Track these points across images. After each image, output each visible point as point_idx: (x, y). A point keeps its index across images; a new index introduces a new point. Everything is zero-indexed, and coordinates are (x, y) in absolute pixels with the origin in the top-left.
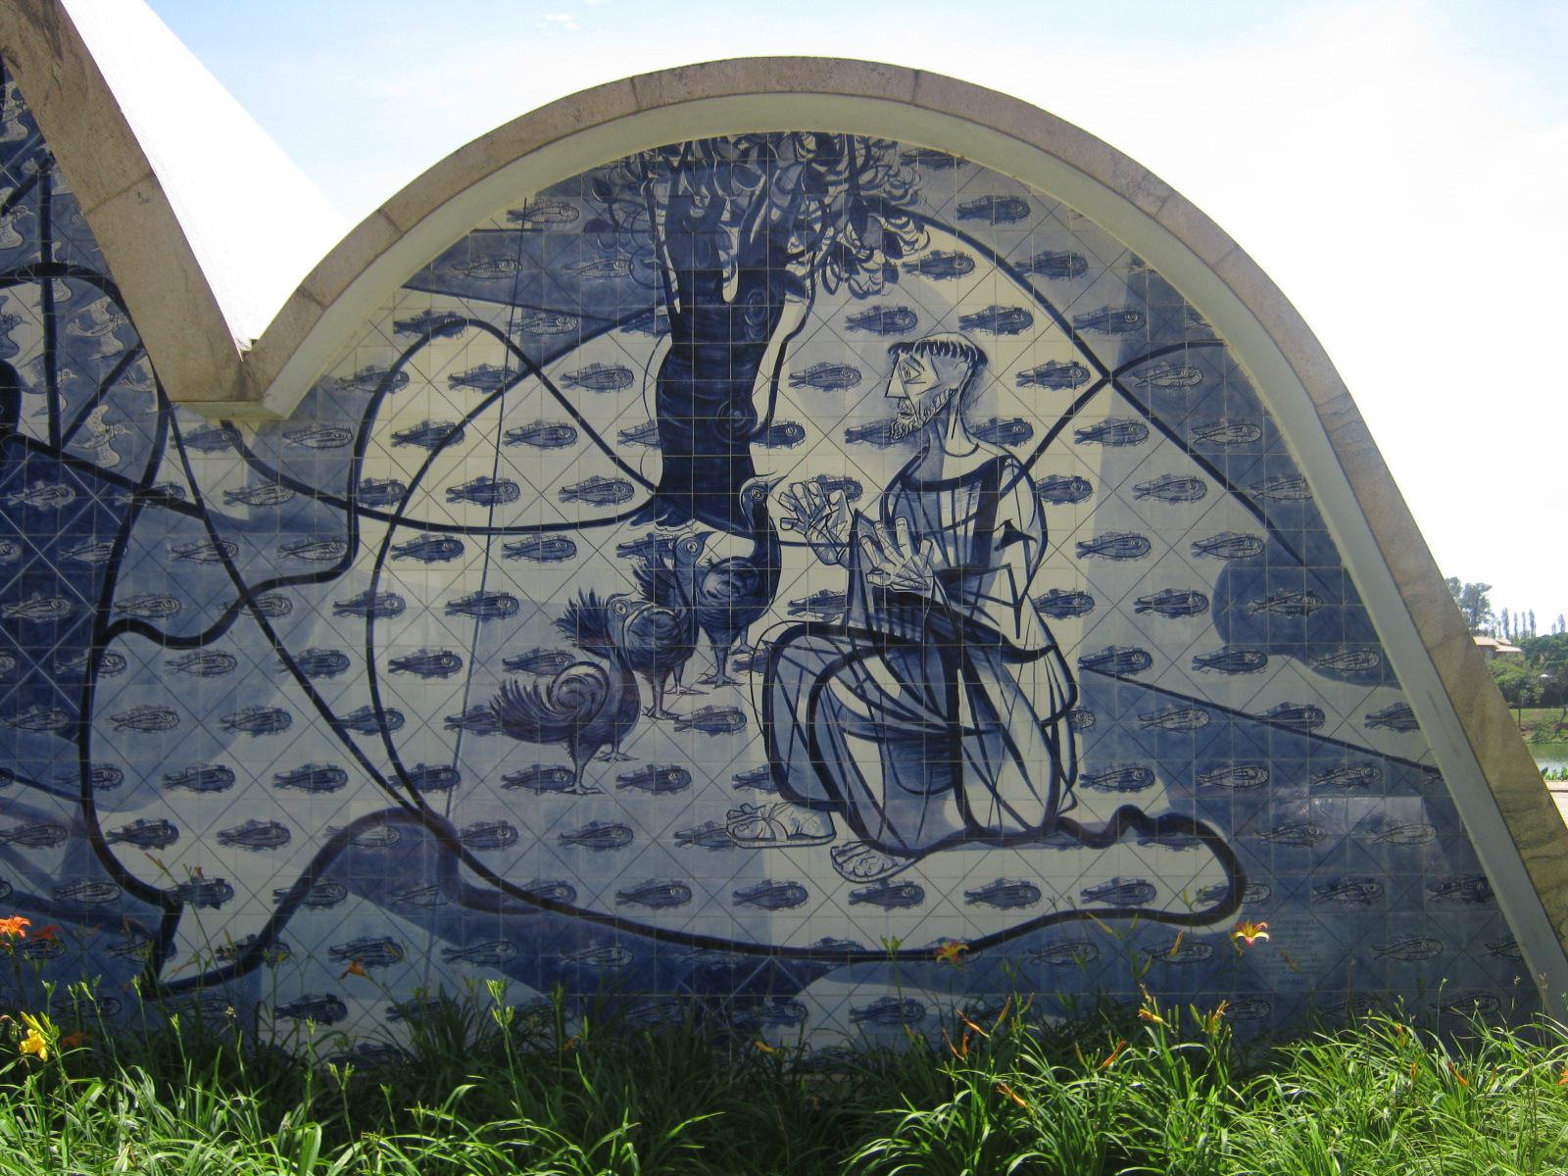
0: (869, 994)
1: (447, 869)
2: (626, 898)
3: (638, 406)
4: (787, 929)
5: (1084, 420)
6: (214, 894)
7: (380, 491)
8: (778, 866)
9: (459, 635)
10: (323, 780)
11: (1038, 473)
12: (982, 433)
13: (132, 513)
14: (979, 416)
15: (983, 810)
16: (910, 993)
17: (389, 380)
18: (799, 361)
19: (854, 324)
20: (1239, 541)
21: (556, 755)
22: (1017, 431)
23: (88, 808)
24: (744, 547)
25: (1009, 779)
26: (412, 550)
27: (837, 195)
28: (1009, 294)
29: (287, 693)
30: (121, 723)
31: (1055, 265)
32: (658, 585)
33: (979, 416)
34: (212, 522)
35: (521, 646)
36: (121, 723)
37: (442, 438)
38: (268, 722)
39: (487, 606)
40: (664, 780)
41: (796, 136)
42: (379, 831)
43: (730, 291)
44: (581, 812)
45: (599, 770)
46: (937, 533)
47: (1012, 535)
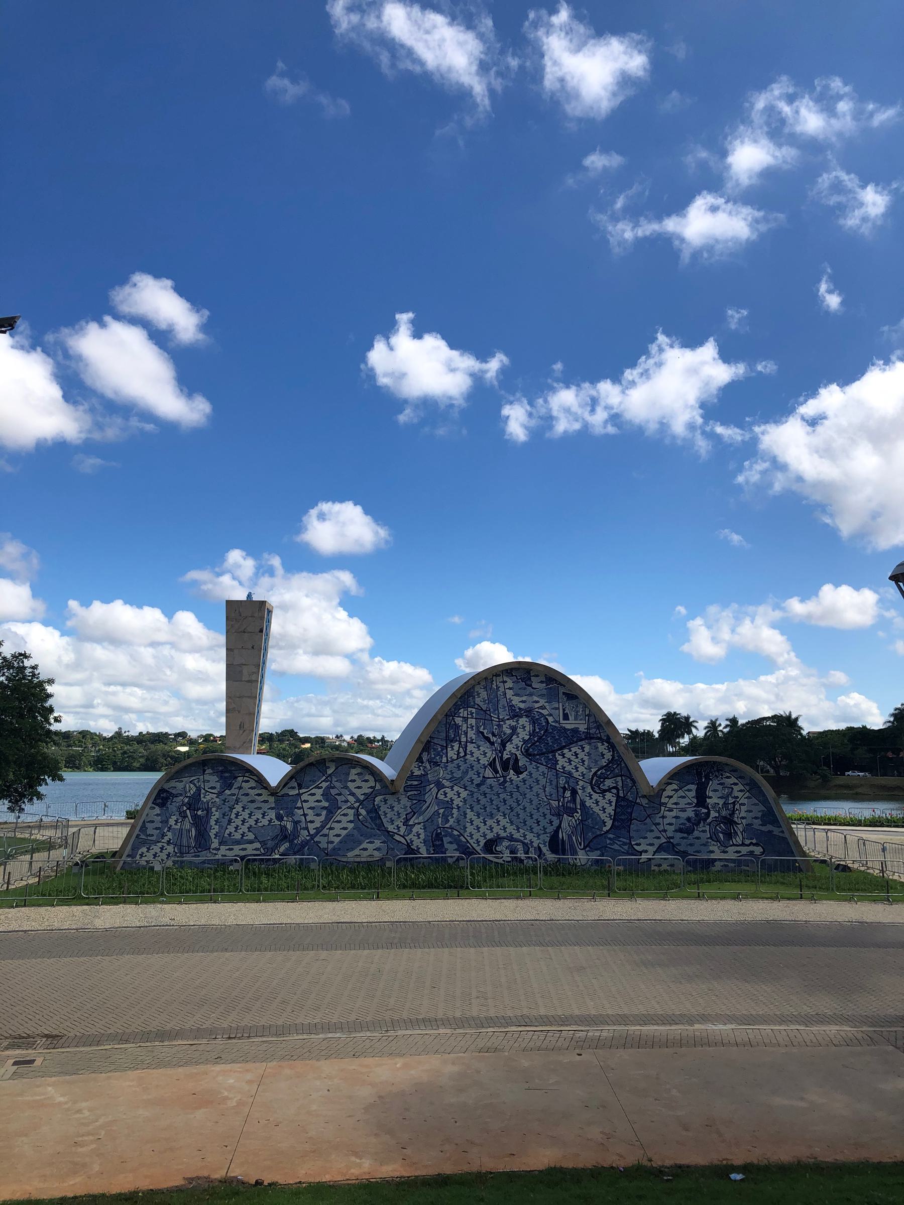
0: (722, 863)
1: (673, 849)
2: (694, 852)
3: (693, 794)
4: (713, 856)
5: (745, 796)
6: (646, 851)
7: (664, 803)
8: (711, 848)
9: (674, 821)
10: (659, 838)
11: (740, 802)
12: (733, 798)
13: (634, 806)
14: (733, 795)
15: (735, 843)
16: (726, 863)
17: (664, 790)
18: (712, 789)
19: (718, 784)
20: (763, 811)
21: (685, 835)
22: (737, 797)
23: (631, 841)
24: (706, 811)
25: (738, 839)
26: (668, 811)
27: (715, 769)
28: (736, 781)
29: (654, 827)
30: (634, 831)
31: (740, 777)
32: (696, 815)
33: (733, 795)
34: (644, 807)
35: (680, 823)
36: (634, 831)
37: (670, 797)
38: (652, 831)
39: (677, 817)
40: (698, 838)
41: (710, 762)
42: (665, 844)
43: (703, 780)
44: (689, 842)
45: (690, 837)
46: (729, 810)
47: (737, 810)
